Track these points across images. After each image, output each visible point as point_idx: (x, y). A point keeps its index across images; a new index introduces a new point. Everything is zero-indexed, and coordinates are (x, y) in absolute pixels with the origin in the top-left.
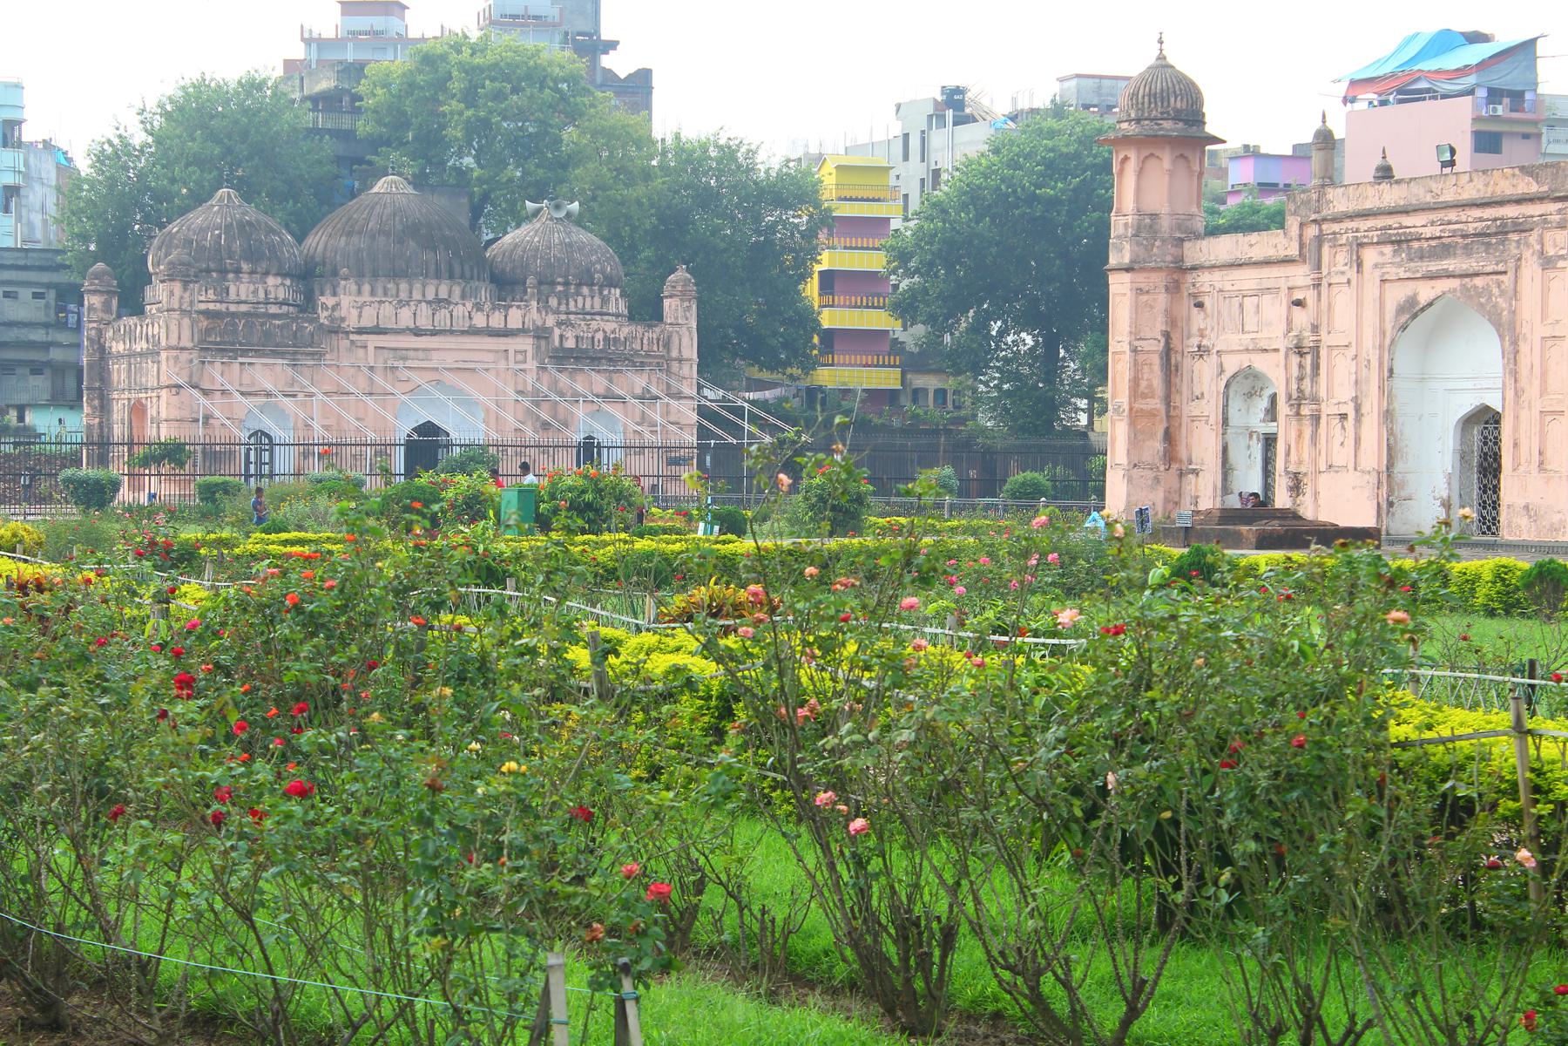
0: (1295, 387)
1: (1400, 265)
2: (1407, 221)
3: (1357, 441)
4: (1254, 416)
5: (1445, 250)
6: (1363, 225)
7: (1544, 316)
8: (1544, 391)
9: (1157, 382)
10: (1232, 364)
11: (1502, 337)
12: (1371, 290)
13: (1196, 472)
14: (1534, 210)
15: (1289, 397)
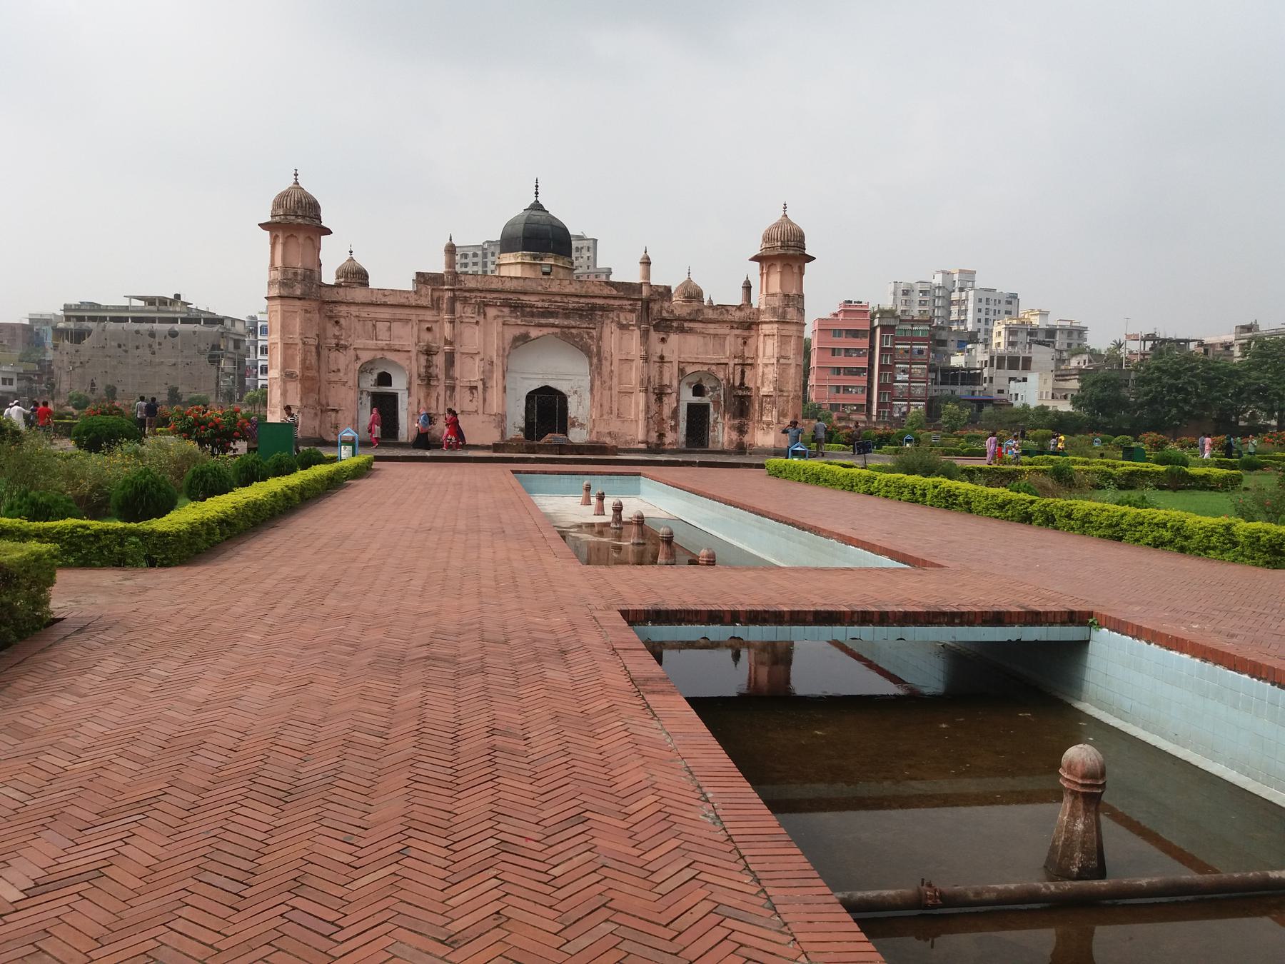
0: (423, 370)
1: (517, 317)
2: (523, 297)
3: (485, 400)
4: (369, 383)
5: (547, 313)
6: (489, 296)
7: (620, 350)
8: (620, 383)
9: (314, 361)
10: (366, 356)
11: (590, 358)
12: (496, 327)
13: (337, 411)
14: (617, 302)
15: (419, 376)
